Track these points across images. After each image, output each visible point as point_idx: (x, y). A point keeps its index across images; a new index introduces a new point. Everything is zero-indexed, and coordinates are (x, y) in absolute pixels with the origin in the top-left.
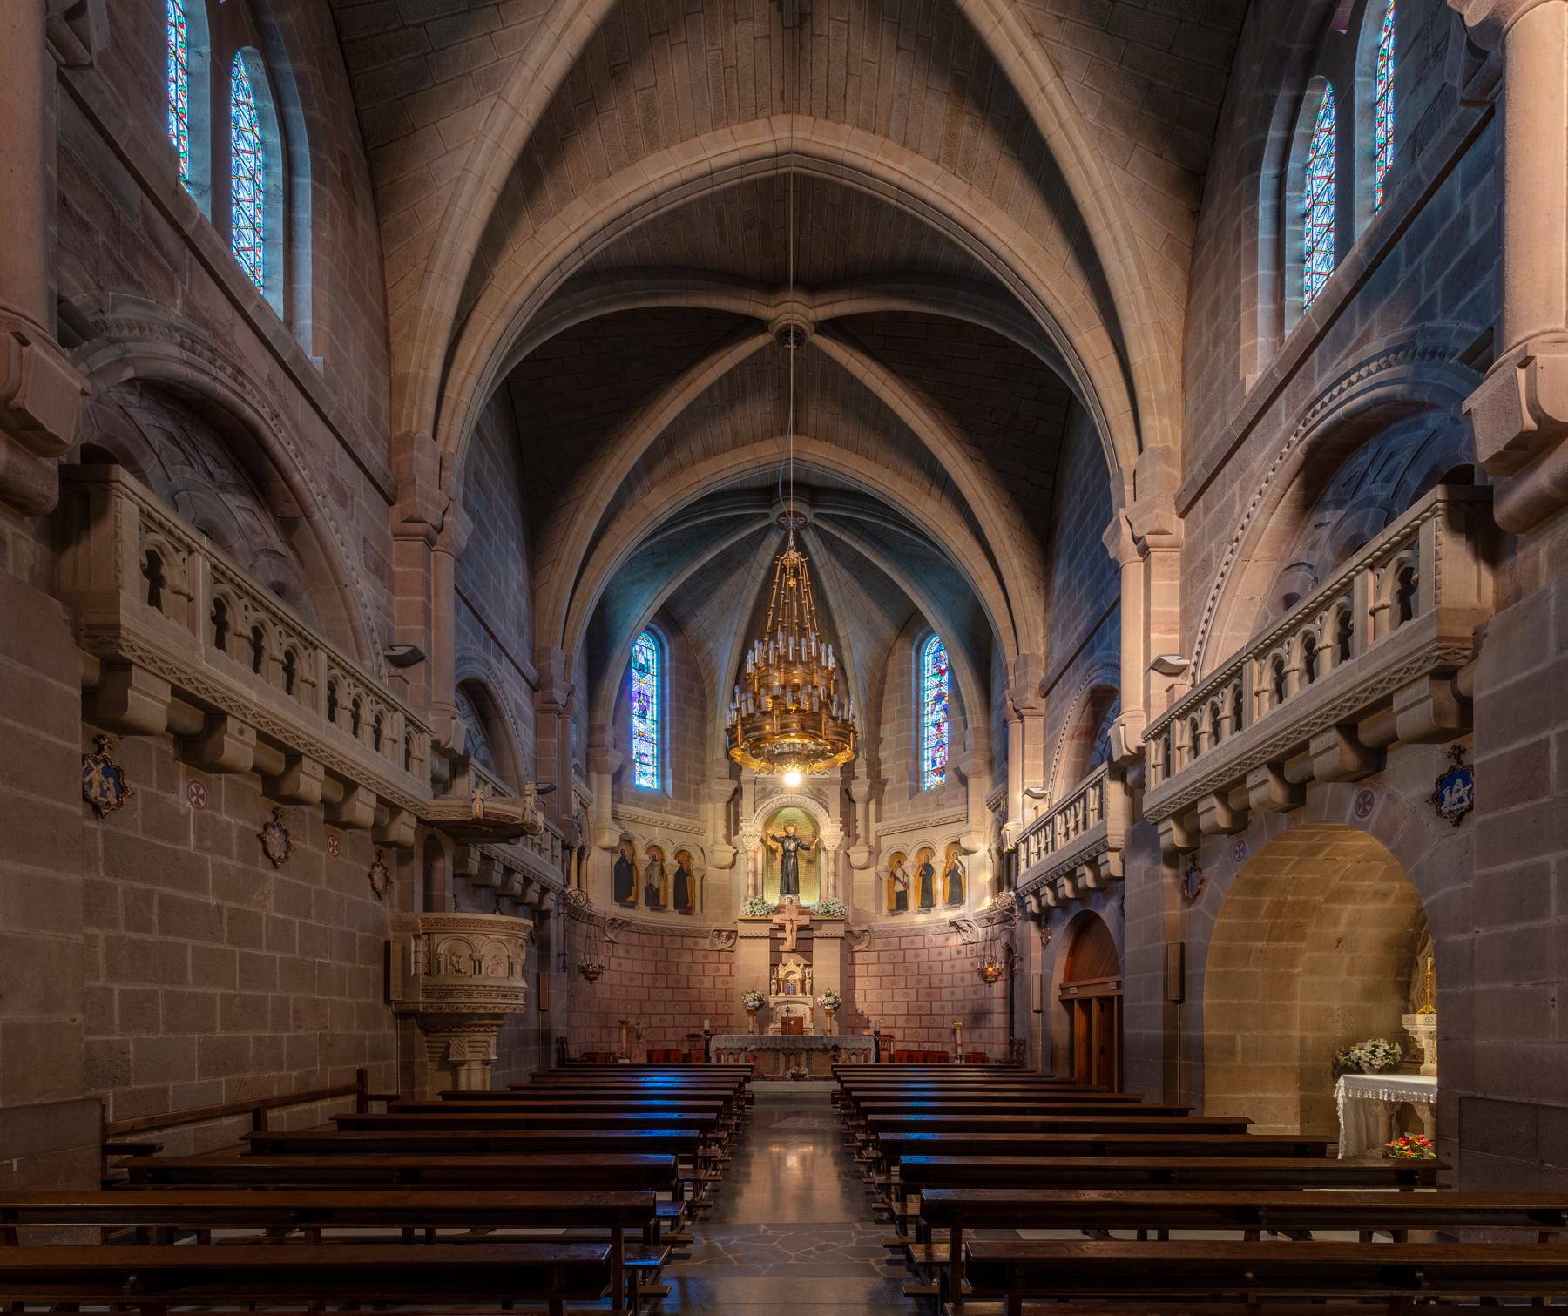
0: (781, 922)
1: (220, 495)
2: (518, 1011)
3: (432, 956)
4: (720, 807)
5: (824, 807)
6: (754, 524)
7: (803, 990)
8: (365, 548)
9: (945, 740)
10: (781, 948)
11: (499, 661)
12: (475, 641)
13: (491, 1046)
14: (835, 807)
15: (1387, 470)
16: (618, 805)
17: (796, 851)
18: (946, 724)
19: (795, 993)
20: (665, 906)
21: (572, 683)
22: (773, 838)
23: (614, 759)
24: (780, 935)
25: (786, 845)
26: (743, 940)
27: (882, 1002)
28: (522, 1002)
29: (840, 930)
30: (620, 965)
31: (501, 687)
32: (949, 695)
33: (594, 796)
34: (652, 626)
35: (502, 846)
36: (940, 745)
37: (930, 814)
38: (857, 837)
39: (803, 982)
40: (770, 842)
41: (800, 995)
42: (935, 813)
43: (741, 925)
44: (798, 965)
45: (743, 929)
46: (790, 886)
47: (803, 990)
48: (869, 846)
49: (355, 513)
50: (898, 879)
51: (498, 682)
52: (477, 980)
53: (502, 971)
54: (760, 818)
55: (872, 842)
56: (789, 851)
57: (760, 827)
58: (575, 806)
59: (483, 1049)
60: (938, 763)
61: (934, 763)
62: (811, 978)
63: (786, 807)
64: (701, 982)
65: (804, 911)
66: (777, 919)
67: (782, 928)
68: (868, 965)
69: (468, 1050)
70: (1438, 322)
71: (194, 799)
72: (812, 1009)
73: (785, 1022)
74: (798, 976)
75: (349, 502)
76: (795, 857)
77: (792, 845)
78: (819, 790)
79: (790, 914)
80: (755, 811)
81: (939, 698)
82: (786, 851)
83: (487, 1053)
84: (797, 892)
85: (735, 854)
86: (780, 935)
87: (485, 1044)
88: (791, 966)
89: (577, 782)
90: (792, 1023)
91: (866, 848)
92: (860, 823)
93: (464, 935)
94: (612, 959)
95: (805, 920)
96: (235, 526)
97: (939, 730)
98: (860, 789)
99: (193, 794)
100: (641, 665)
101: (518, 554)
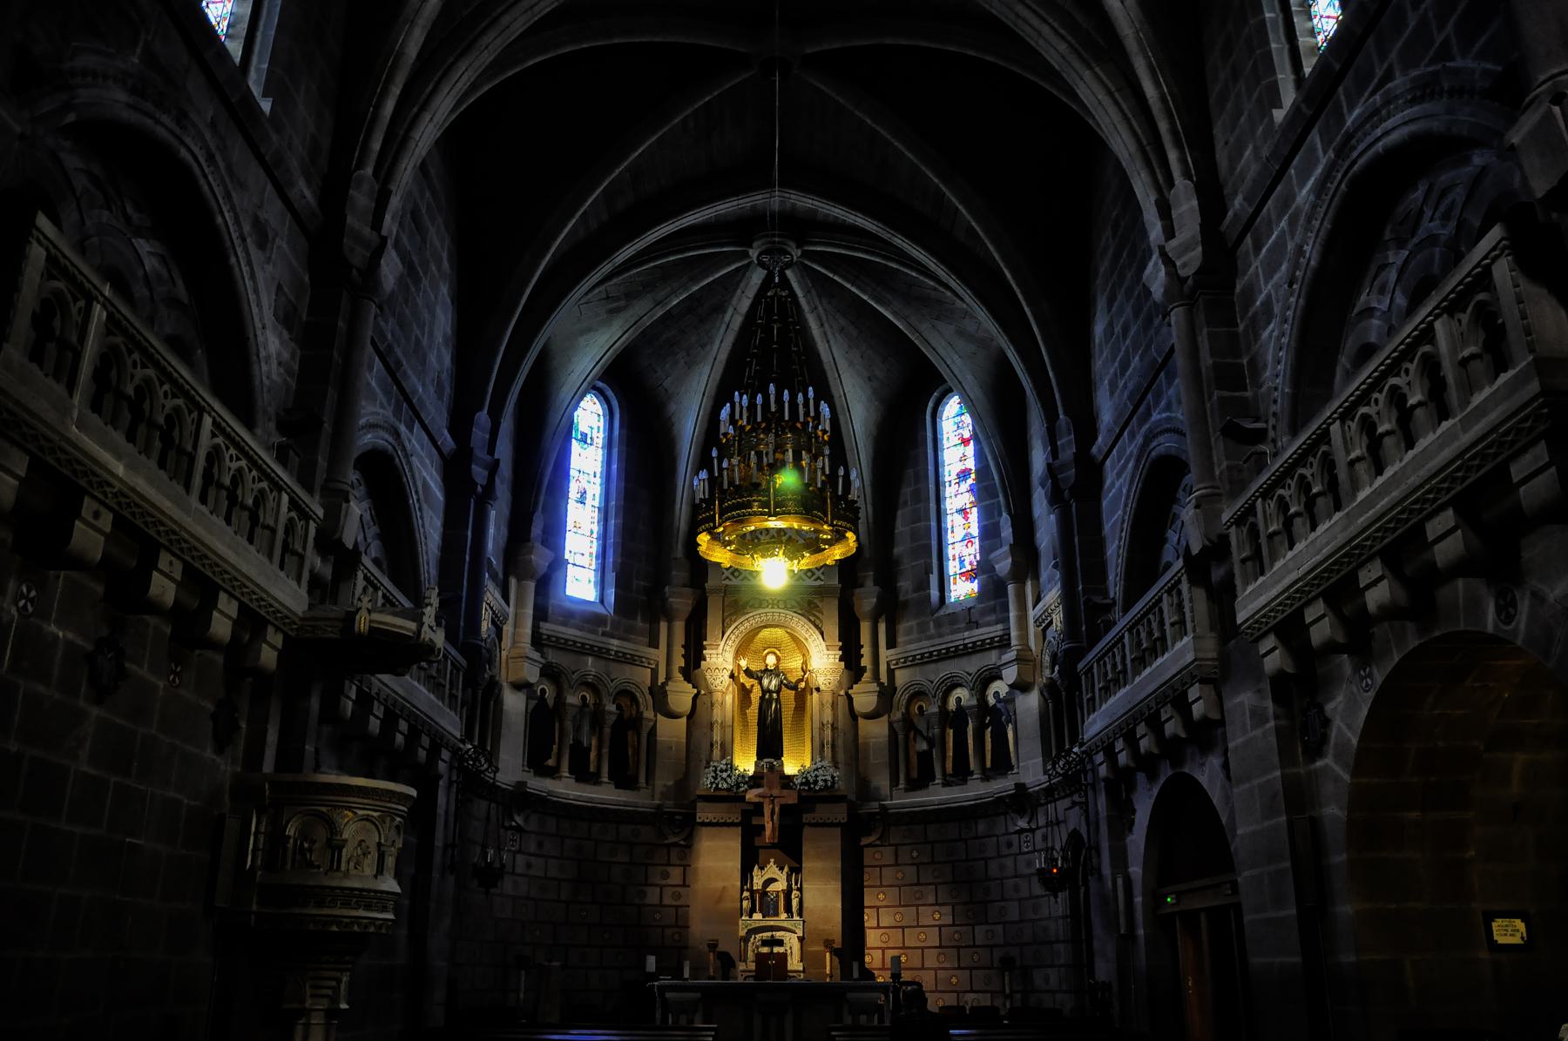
0: (757, 800)
1: (133, 240)
2: (383, 931)
3: (276, 837)
4: (679, 627)
5: (817, 626)
6: (729, 264)
7: (788, 909)
8: (276, 295)
9: (975, 531)
11: (411, 429)
12: (385, 404)
13: (343, 987)
14: (833, 629)
15: (1442, 209)
16: (542, 624)
17: (778, 691)
18: (975, 510)
19: (777, 914)
20: (598, 774)
21: (496, 457)
22: (748, 672)
23: (539, 558)
24: (755, 821)
25: (765, 682)
27: (903, 928)
28: (390, 916)
29: (840, 813)
30: (529, 866)
31: (409, 463)
32: (977, 472)
33: (511, 610)
34: (600, 384)
35: (385, 678)
36: (968, 539)
37: (960, 636)
38: (864, 669)
40: (743, 679)
41: (784, 916)
42: (966, 634)
43: (700, 805)
44: (781, 869)
45: (704, 813)
46: (770, 747)
47: (788, 909)
48: (880, 684)
49: (273, 256)
50: (920, 733)
51: (406, 456)
52: (335, 881)
53: (369, 868)
54: (730, 643)
55: (884, 678)
56: (770, 692)
57: (729, 656)
58: (485, 626)
59: (330, 992)
60: (967, 563)
61: (962, 562)
62: (800, 890)
63: (765, 627)
65: (787, 781)
66: (752, 795)
67: (758, 809)
68: (881, 867)
69: (309, 991)
70: (1458, 63)
71: (22, 603)
72: (801, 939)
73: (760, 958)
74: (781, 885)
75: (269, 245)
76: (778, 701)
77: (774, 682)
78: (810, 603)
79: (771, 788)
81: (963, 475)
82: (765, 691)
83: (335, 1000)
84: (778, 755)
85: (695, 698)
86: (755, 821)
87: (334, 983)
88: (772, 870)
89: (492, 595)
91: (874, 687)
92: (866, 651)
93: (324, 809)
94: (519, 856)
95: (791, 798)
96: (140, 273)
97: (966, 518)
98: (867, 599)
99: (22, 596)
100: (582, 434)
101: (449, 300)
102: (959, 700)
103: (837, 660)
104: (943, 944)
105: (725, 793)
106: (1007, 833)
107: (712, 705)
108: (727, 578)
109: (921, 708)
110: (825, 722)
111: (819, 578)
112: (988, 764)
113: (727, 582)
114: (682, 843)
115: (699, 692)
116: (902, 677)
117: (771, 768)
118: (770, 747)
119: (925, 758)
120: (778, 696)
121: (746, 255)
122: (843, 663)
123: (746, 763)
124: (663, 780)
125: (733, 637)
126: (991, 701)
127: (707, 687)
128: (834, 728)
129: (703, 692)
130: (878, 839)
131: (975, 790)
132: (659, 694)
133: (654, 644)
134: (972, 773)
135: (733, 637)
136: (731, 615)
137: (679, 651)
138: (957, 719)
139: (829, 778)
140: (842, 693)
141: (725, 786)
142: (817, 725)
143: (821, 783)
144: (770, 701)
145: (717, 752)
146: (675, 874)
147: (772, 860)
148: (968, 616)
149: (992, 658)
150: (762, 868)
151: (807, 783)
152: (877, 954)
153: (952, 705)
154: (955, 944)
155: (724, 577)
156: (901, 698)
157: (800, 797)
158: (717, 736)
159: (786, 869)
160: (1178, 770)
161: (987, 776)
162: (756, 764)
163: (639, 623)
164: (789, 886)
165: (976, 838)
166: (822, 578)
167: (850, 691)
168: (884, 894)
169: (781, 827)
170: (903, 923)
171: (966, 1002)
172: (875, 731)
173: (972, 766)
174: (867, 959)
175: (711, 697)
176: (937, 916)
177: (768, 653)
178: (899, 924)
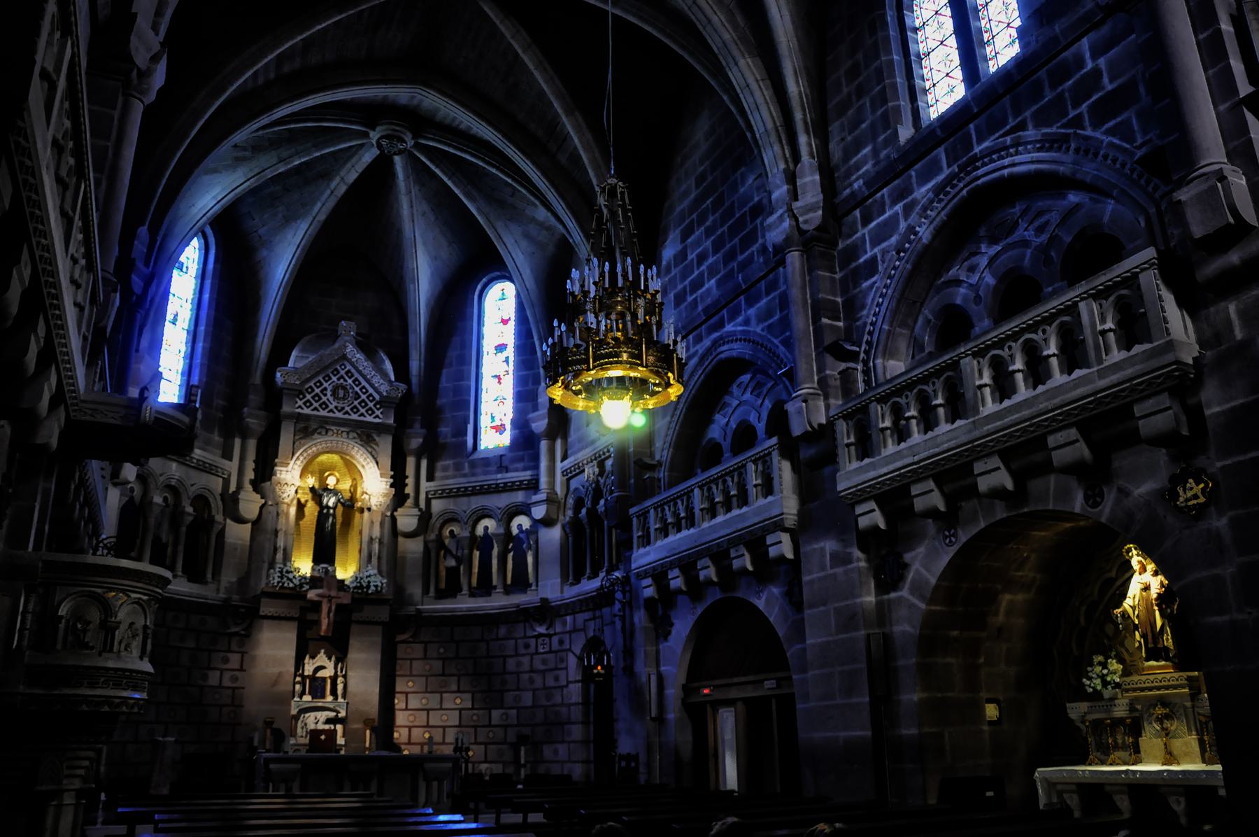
4: (252, 444)
5: (373, 456)
10: (309, 634)
14: (387, 461)
26: (265, 622)
27: (428, 710)
29: (383, 614)
39: (334, 679)
44: (330, 659)
45: (267, 608)
46: (324, 553)
48: (420, 510)
54: (299, 462)
56: (328, 507)
64: (205, 677)
66: (312, 595)
68: (411, 660)
74: (328, 673)
80: (293, 455)
84: (332, 562)
88: (321, 659)
90: (323, 737)
102: (486, 528)
103: (388, 487)
104: (463, 723)
105: (287, 591)
106: (525, 637)
107: (278, 514)
108: (300, 407)
109: (452, 532)
110: (374, 537)
111: (377, 416)
112: (509, 581)
113: (299, 410)
114: (243, 632)
115: (266, 503)
116: (437, 506)
117: (327, 571)
118: (324, 553)
119: (453, 573)
120: (334, 511)
121: (366, 135)
122: (393, 489)
123: (304, 565)
124: (229, 577)
125: (301, 458)
126: (515, 531)
127: (274, 499)
128: (381, 543)
129: (270, 503)
130: (411, 637)
131: (498, 601)
132: (231, 503)
133: (228, 455)
134: (495, 587)
135: (301, 458)
136: (300, 438)
137: (250, 465)
138: (485, 543)
139: (380, 584)
140: (389, 514)
141: (291, 585)
142: (365, 538)
143: (373, 588)
144: (328, 515)
145: (279, 556)
146: (234, 659)
147: (323, 651)
148: (499, 461)
149: (519, 497)
150: (313, 657)
151: (361, 587)
152: (405, 732)
153: (480, 530)
154: (472, 724)
155: (297, 405)
156: (435, 522)
157: (353, 599)
158: (281, 543)
159: (333, 659)
160: (729, 595)
161: (508, 590)
162: (313, 569)
163: (217, 438)
164: (336, 673)
165: (498, 639)
166: (381, 416)
167: (395, 513)
168: (413, 682)
169: (335, 622)
170: (428, 707)
171: (480, 770)
172: (413, 548)
173: (495, 582)
174: (396, 735)
175: (278, 508)
176: (458, 701)
177: (329, 475)
178: (425, 707)
